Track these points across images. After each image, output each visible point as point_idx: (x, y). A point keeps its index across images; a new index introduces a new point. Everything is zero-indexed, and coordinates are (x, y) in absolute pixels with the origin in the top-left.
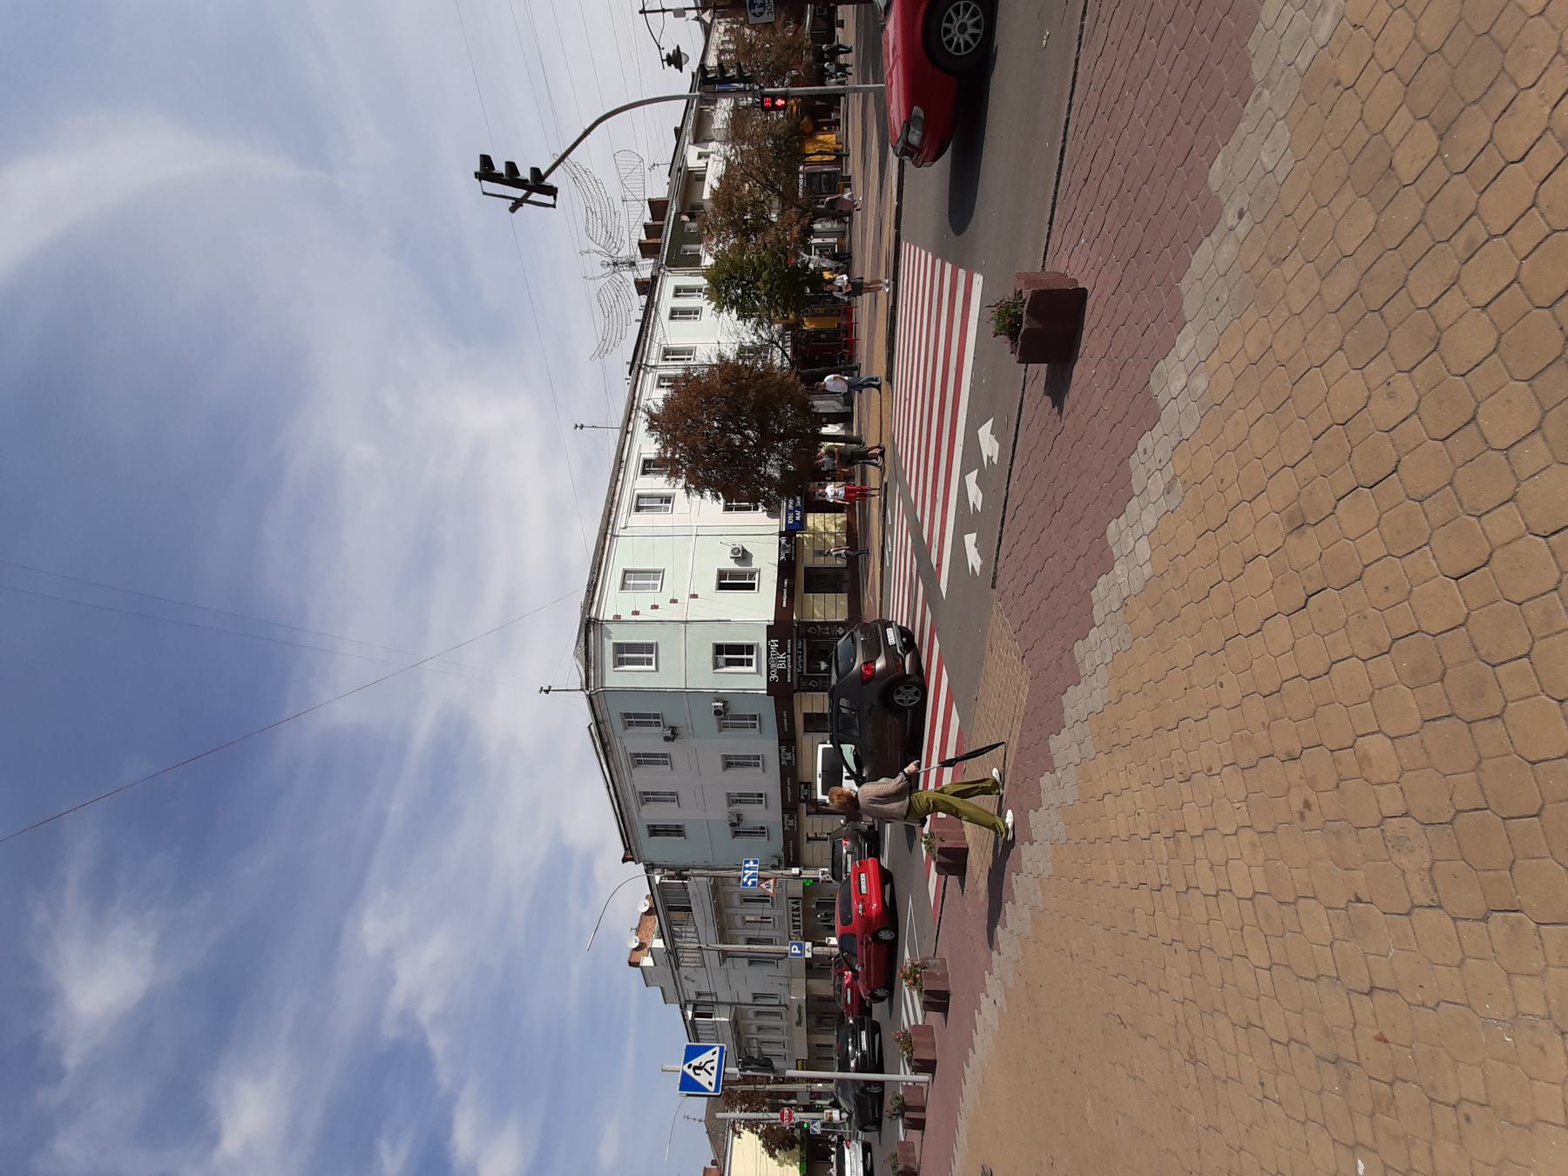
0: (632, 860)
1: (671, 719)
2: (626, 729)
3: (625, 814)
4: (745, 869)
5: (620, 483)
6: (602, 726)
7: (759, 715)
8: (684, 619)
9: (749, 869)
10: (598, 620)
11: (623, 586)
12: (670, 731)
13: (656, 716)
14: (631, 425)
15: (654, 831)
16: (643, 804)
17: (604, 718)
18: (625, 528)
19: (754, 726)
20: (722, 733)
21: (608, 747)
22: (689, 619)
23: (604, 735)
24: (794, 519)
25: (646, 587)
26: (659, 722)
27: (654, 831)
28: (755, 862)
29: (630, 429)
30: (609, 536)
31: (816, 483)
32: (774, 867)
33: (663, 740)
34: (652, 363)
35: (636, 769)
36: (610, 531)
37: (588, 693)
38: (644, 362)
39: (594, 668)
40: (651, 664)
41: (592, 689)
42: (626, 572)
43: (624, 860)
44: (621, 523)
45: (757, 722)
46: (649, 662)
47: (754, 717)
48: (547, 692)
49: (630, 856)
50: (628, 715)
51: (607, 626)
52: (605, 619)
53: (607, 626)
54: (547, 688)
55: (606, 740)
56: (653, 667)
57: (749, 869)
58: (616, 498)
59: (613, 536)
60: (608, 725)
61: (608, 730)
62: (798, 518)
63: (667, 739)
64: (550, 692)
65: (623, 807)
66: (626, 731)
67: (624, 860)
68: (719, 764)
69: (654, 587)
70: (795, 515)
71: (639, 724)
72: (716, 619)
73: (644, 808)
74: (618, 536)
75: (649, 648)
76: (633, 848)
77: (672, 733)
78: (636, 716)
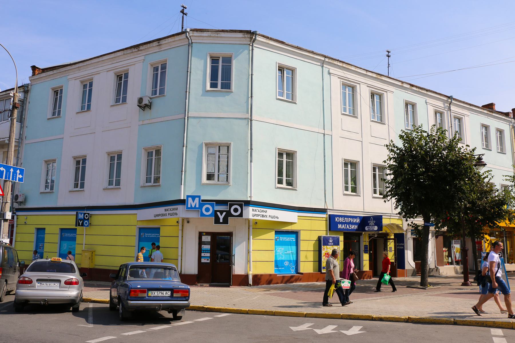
0: (34, 74)
1: (158, 103)
2: (152, 65)
3: (74, 67)
4: (15, 170)
5: (364, 72)
6: (155, 44)
7: (159, 186)
8: (253, 118)
9: (15, 173)
10: (253, 42)
11: (281, 69)
12: (147, 103)
13: (162, 92)
14: (408, 86)
15: (57, 93)
16: (82, 82)
17: (161, 46)
18: (329, 73)
19: (148, 180)
20: (143, 151)
21: (136, 50)
22: (253, 122)
23: (145, 47)
24: (340, 223)
25: (281, 86)
26: (156, 94)
27: (57, 93)
28: (21, 180)
29: (405, 85)
30: (323, 59)
31: (368, 244)
32: (15, 198)
33: (139, 96)
34: (453, 108)
35: (113, 74)
36: (327, 60)
37: (188, 30)
38: (453, 102)
39: (210, 36)
40: (211, 87)
41: (191, 35)
42: (293, 71)
43: (34, 68)
44: (333, 70)
45: (152, 183)
46: (214, 85)
47: (157, 180)
48: (182, 12)
49: (37, 72)
50: (164, 67)
51: (246, 52)
52: (254, 48)
53: (246, 52)
54: (185, 12)
55: (141, 48)
56: (208, 88)
57: (15, 173)
58: (353, 68)
59: (323, 63)
60: (156, 49)
61: (150, 50)
62: (340, 226)
63: (140, 100)
64: (182, 14)
65: (80, 65)
66: (149, 66)
67: (34, 68)
68: (115, 148)
69: (281, 94)
70: (342, 223)
71: (155, 76)
72: (253, 148)
73: (78, 82)
74: (323, 67)
75: (227, 86)
76: (44, 75)
77: (146, 105)
78: (163, 74)
